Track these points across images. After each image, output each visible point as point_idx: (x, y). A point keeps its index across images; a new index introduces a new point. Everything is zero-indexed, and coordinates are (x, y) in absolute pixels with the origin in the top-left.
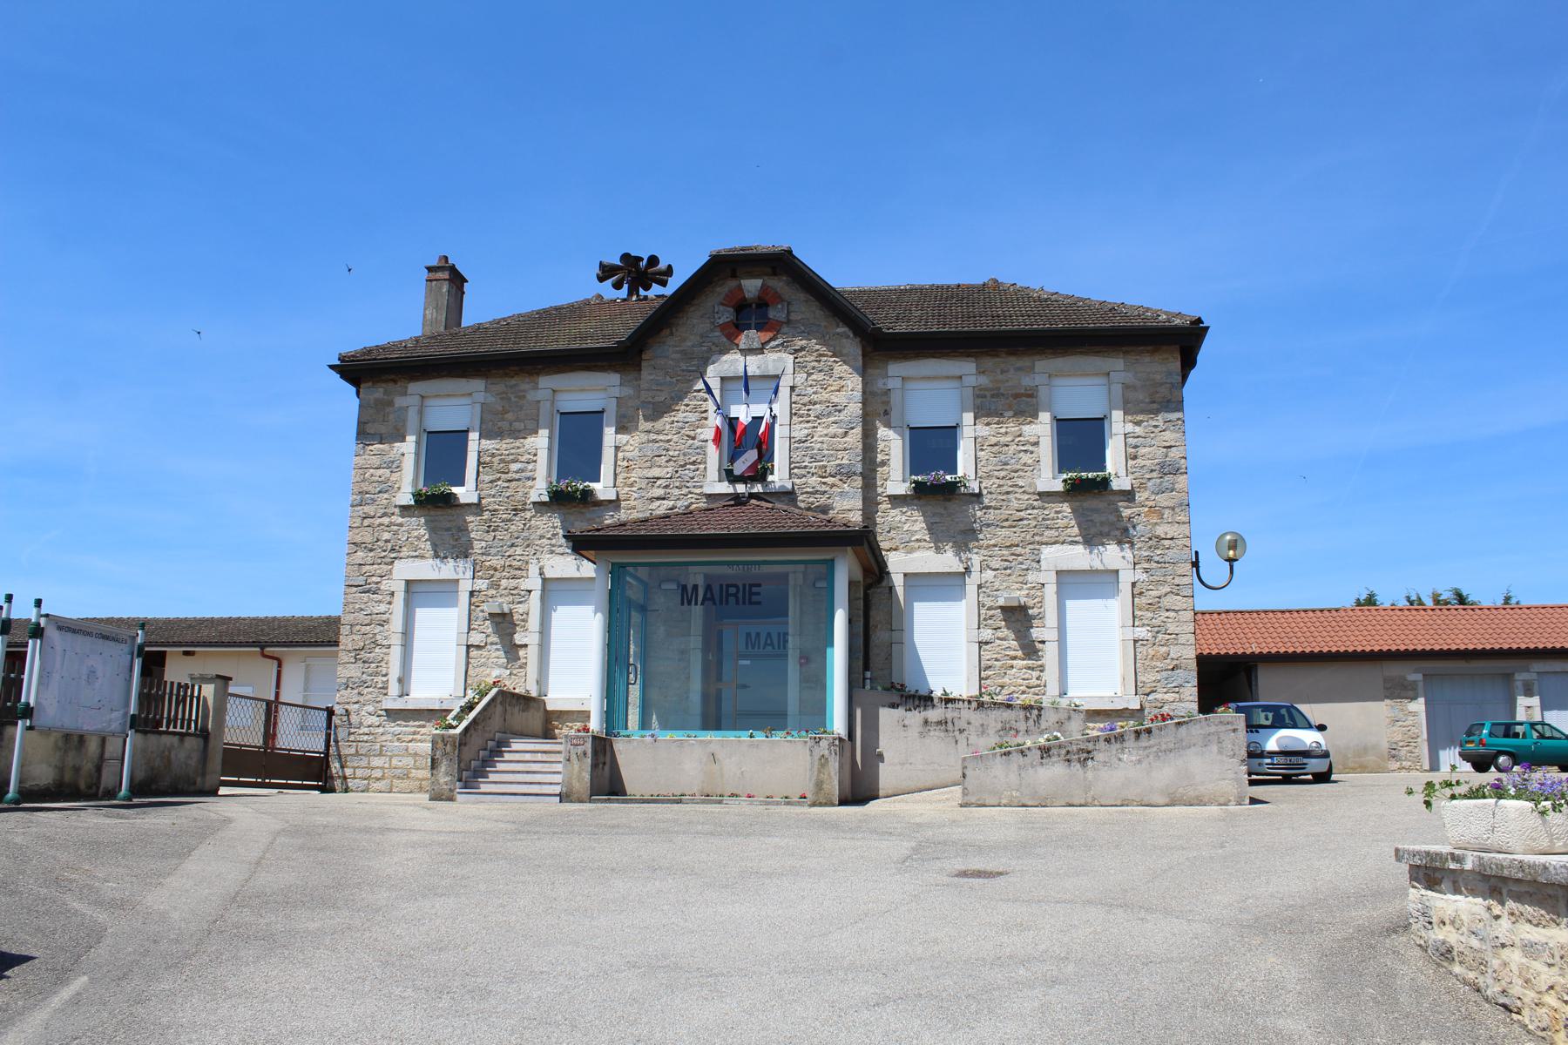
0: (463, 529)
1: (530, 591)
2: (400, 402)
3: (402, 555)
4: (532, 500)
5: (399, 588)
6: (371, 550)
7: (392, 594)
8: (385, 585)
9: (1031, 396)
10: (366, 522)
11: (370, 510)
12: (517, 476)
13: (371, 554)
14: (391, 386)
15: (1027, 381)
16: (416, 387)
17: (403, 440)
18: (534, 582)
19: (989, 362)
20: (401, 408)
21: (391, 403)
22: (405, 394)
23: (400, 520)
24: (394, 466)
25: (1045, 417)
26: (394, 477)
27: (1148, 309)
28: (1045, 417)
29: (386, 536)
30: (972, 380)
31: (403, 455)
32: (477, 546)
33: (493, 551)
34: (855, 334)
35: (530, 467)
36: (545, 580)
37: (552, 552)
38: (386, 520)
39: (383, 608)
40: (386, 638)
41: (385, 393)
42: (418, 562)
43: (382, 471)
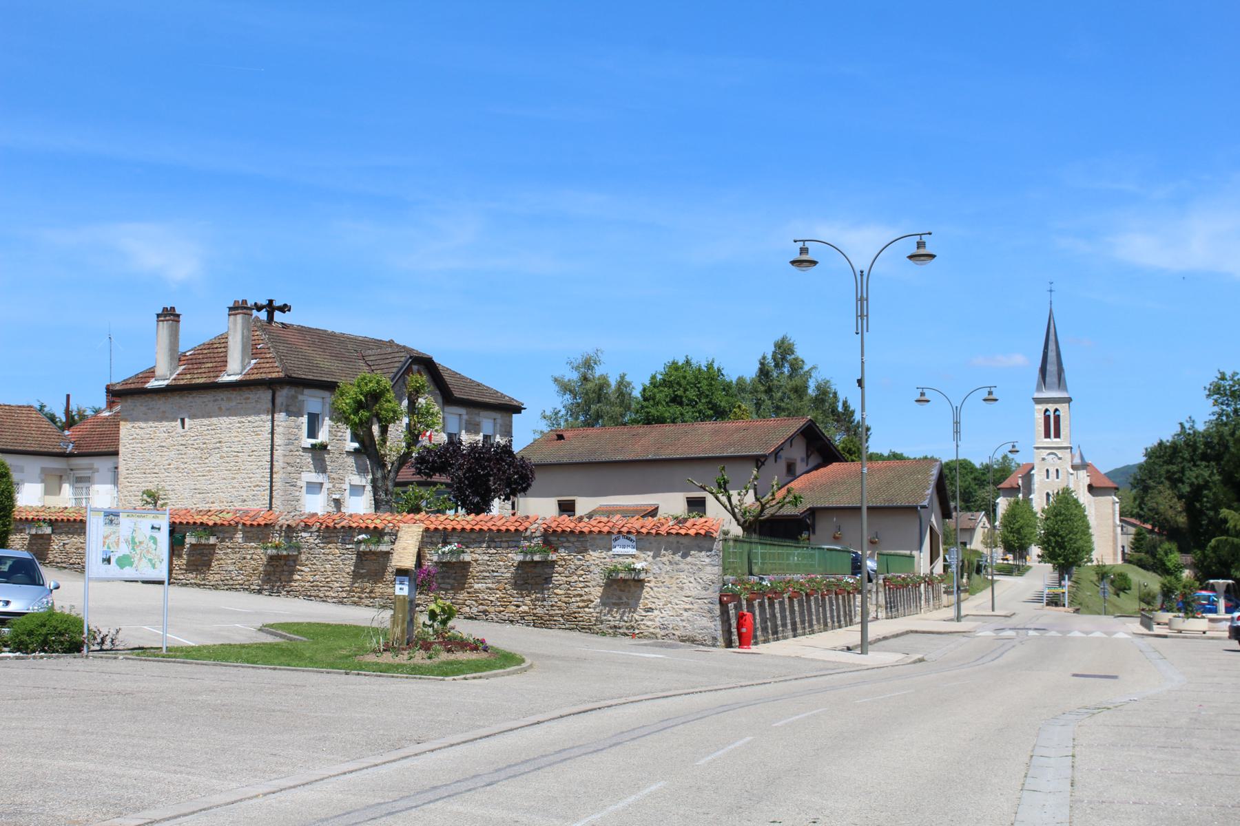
0: (324, 461)
1: (345, 490)
2: (300, 397)
3: (304, 470)
4: (346, 450)
5: (304, 485)
6: (293, 467)
7: (301, 487)
8: (299, 483)
9: (478, 425)
10: (291, 453)
11: (291, 447)
12: (340, 438)
13: (293, 468)
14: (297, 389)
15: (477, 419)
16: (307, 391)
17: (302, 416)
18: (347, 486)
19: (469, 410)
20: (300, 401)
21: (297, 398)
22: (302, 394)
23: (303, 454)
24: (299, 427)
25: (481, 434)
26: (299, 433)
27: (497, 392)
28: (481, 434)
29: (298, 461)
30: (465, 417)
31: (302, 423)
32: (329, 468)
33: (334, 471)
34: (441, 394)
35: (344, 434)
36: (351, 485)
37: (352, 473)
38: (297, 453)
39: (297, 494)
40: (300, 507)
41: (295, 391)
42: (310, 474)
43: (295, 430)
